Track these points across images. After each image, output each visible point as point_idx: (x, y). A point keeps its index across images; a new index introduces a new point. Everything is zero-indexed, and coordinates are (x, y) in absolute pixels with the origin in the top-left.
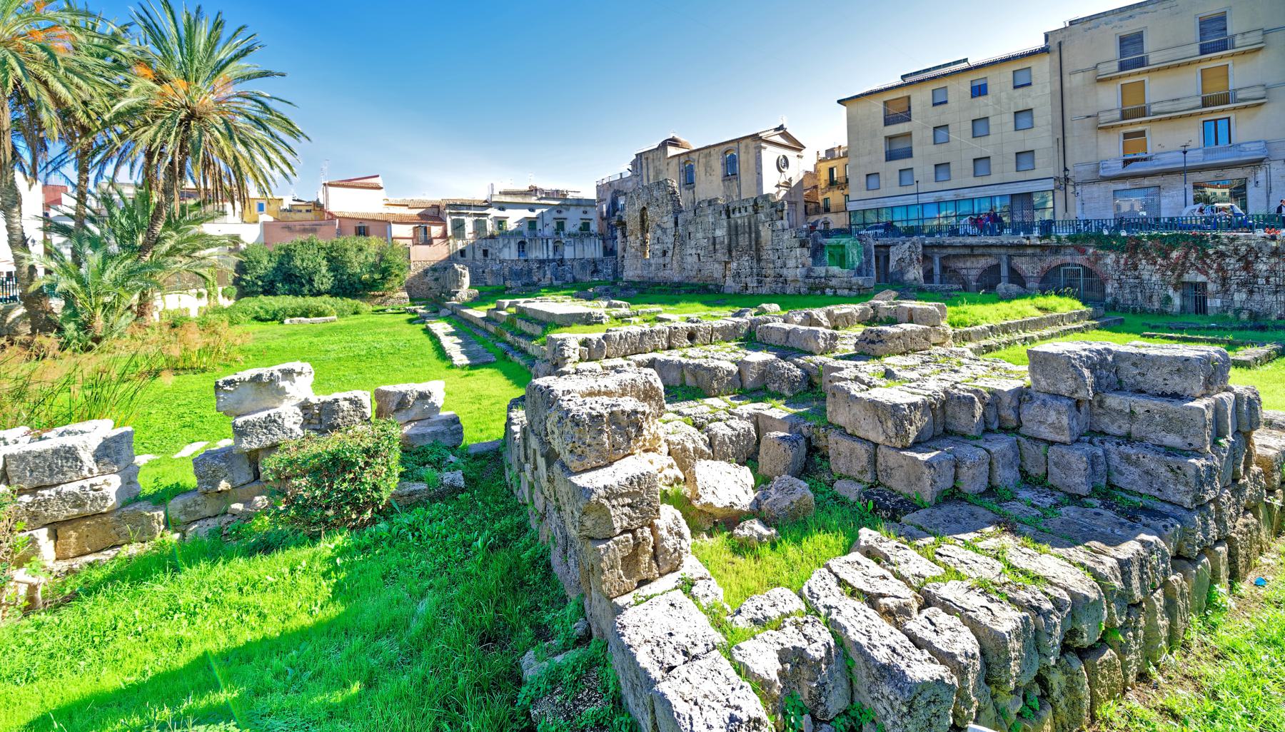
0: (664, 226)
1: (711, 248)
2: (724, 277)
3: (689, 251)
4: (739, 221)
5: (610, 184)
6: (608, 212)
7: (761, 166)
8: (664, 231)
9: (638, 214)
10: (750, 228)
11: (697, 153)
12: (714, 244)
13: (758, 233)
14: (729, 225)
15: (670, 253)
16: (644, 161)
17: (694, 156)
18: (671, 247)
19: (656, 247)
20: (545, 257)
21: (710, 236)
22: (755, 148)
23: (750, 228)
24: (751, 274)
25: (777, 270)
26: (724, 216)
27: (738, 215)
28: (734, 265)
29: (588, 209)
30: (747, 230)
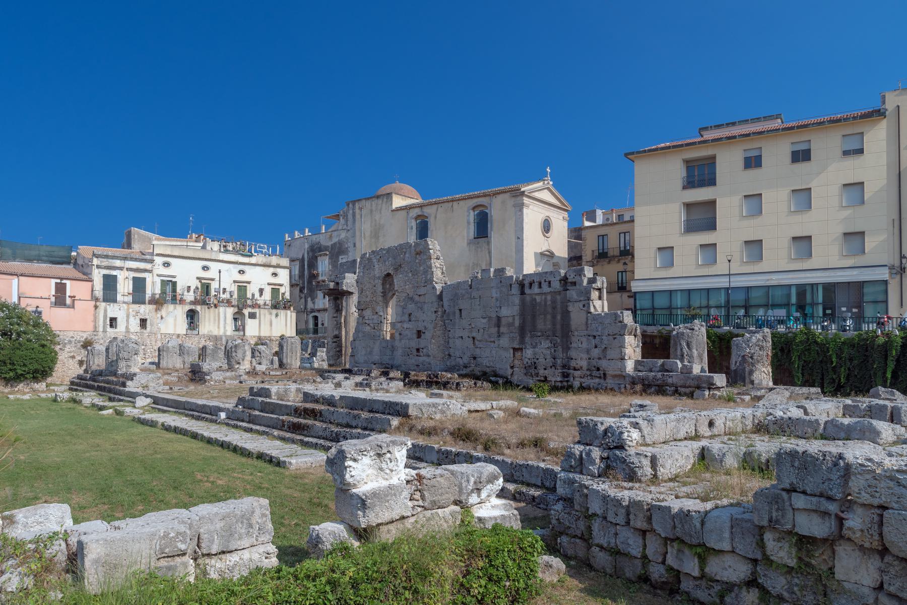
0: (422, 299)
1: (494, 330)
3: (459, 333)
4: (538, 299)
6: (301, 275)
7: (521, 229)
9: (379, 283)
10: (554, 308)
11: (435, 207)
12: (499, 326)
13: (566, 314)
14: (523, 304)
15: (428, 335)
16: (357, 211)
18: (430, 326)
19: (405, 326)
20: (221, 333)
21: (494, 315)
22: (514, 206)
23: (554, 308)
24: (554, 366)
25: (594, 362)
27: (536, 289)
28: (529, 353)
29: (278, 270)
30: (550, 310)
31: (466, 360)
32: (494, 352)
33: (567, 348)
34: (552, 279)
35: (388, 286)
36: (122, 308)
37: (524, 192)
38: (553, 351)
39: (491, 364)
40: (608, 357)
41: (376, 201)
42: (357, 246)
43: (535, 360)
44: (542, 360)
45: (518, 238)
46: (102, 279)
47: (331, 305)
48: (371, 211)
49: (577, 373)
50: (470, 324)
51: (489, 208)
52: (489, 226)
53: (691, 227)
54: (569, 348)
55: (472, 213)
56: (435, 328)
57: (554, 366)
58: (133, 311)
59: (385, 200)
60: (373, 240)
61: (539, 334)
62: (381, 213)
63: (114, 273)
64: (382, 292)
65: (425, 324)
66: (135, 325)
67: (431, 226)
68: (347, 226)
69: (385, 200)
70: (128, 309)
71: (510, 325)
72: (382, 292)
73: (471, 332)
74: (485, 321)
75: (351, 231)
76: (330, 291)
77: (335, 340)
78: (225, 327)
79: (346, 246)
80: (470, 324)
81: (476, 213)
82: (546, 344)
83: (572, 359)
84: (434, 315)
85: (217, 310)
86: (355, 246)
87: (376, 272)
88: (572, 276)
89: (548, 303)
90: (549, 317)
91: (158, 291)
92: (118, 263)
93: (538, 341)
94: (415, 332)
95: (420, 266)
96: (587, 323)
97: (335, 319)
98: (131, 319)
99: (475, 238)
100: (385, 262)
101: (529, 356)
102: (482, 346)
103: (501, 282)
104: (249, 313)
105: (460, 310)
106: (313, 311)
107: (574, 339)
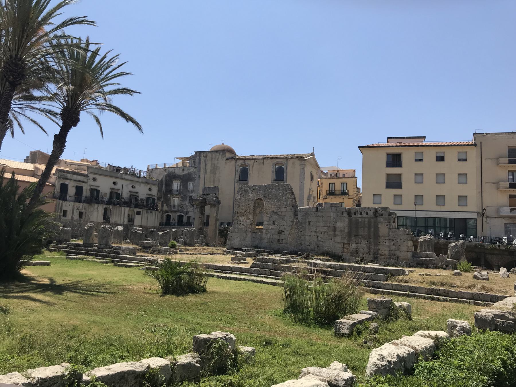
0: (283, 214)
1: (332, 233)
2: (342, 252)
4: (360, 220)
5: (165, 169)
8: (282, 217)
11: (253, 161)
13: (377, 229)
14: (350, 222)
15: (287, 233)
17: (251, 163)
18: (288, 228)
19: (271, 227)
21: (331, 226)
25: (392, 252)
26: (345, 215)
28: (354, 246)
30: (367, 226)
31: (312, 247)
32: (331, 244)
33: (377, 244)
34: (368, 211)
35: (257, 205)
36: (70, 205)
38: (368, 246)
39: (330, 250)
40: (400, 250)
41: (215, 153)
42: (201, 176)
43: (357, 249)
44: (361, 250)
45: (301, 183)
46: (60, 186)
47: (199, 211)
48: (212, 159)
49: (383, 257)
51: (285, 165)
52: (285, 174)
53: (389, 185)
54: (378, 245)
55: (275, 167)
56: (291, 229)
57: (369, 253)
58: (76, 207)
59: (221, 154)
60: (212, 175)
61: (360, 237)
62: (218, 160)
63: (67, 182)
64: (253, 208)
65: (285, 227)
66: (76, 216)
67: (250, 172)
68: (195, 165)
69: (221, 154)
70: (74, 206)
71: (341, 231)
75: (198, 168)
77: (199, 231)
78: (124, 219)
79: (194, 176)
81: (277, 167)
82: (364, 242)
83: (380, 250)
84: (291, 224)
85: (120, 208)
86: (199, 176)
87: (250, 197)
88: (381, 211)
89: (366, 222)
90: (366, 229)
91: (88, 194)
92: (69, 176)
93: (359, 240)
94: (277, 230)
95: (283, 197)
96: (389, 234)
97: (200, 219)
98: (75, 212)
100: (257, 192)
101: (354, 247)
103: (337, 210)
104: (137, 211)
105: (309, 222)
106: (167, 212)
107: (381, 240)
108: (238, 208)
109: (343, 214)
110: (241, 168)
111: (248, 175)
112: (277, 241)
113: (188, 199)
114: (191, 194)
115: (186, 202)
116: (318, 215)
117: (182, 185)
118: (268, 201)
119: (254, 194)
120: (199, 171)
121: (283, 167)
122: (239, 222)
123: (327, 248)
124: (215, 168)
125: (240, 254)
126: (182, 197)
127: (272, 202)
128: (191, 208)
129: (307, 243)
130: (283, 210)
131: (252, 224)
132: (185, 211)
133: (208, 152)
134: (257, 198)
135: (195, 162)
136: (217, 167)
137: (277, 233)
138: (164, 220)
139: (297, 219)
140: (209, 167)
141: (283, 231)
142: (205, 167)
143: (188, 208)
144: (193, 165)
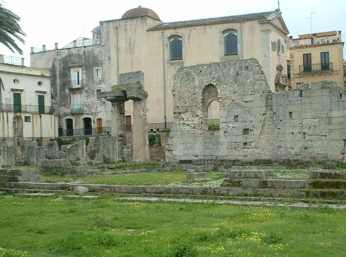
9: (199, 92)
11: (188, 29)
12: (330, 123)
15: (256, 132)
19: (231, 125)
32: (325, 143)
37: (270, 20)
47: (116, 109)
48: (126, 30)
50: (302, 123)
52: (239, 46)
55: (223, 35)
56: (263, 126)
62: (135, 32)
64: (202, 99)
65: (253, 123)
72: (202, 99)
73: (302, 129)
74: (317, 120)
76: (117, 98)
77: (120, 138)
79: (101, 59)
80: (302, 123)
81: (226, 35)
84: (263, 118)
86: (109, 59)
87: (196, 83)
94: (242, 130)
99: (225, 55)
102: (312, 139)
105: (291, 113)
106: (67, 115)
108: (178, 101)
109: (341, 98)
110: (171, 40)
111: (184, 51)
112: (241, 145)
113: (96, 93)
114: (99, 86)
115: (94, 98)
116: (303, 102)
117: (84, 74)
118: (224, 86)
119: (202, 78)
120: (109, 50)
121: (236, 34)
122: (182, 122)
123: (319, 149)
124: (133, 43)
125: (192, 168)
126: (86, 92)
127: (231, 88)
128: (101, 106)
129: (288, 145)
130: (249, 98)
131: (202, 123)
132: (93, 111)
133: (120, 20)
134: (207, 84)
135: (101, 38)
136: (135, 41)
137: (241, 133)
138: (65, 128)
139: (271, 110)
140: (123, 44)
141: (251, 130)
142: (117, 43)
143: (97, 107)
144: (98, 43)
